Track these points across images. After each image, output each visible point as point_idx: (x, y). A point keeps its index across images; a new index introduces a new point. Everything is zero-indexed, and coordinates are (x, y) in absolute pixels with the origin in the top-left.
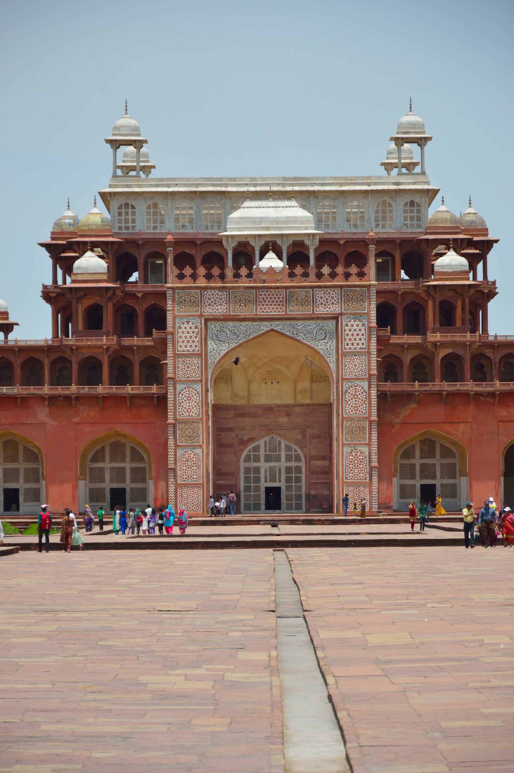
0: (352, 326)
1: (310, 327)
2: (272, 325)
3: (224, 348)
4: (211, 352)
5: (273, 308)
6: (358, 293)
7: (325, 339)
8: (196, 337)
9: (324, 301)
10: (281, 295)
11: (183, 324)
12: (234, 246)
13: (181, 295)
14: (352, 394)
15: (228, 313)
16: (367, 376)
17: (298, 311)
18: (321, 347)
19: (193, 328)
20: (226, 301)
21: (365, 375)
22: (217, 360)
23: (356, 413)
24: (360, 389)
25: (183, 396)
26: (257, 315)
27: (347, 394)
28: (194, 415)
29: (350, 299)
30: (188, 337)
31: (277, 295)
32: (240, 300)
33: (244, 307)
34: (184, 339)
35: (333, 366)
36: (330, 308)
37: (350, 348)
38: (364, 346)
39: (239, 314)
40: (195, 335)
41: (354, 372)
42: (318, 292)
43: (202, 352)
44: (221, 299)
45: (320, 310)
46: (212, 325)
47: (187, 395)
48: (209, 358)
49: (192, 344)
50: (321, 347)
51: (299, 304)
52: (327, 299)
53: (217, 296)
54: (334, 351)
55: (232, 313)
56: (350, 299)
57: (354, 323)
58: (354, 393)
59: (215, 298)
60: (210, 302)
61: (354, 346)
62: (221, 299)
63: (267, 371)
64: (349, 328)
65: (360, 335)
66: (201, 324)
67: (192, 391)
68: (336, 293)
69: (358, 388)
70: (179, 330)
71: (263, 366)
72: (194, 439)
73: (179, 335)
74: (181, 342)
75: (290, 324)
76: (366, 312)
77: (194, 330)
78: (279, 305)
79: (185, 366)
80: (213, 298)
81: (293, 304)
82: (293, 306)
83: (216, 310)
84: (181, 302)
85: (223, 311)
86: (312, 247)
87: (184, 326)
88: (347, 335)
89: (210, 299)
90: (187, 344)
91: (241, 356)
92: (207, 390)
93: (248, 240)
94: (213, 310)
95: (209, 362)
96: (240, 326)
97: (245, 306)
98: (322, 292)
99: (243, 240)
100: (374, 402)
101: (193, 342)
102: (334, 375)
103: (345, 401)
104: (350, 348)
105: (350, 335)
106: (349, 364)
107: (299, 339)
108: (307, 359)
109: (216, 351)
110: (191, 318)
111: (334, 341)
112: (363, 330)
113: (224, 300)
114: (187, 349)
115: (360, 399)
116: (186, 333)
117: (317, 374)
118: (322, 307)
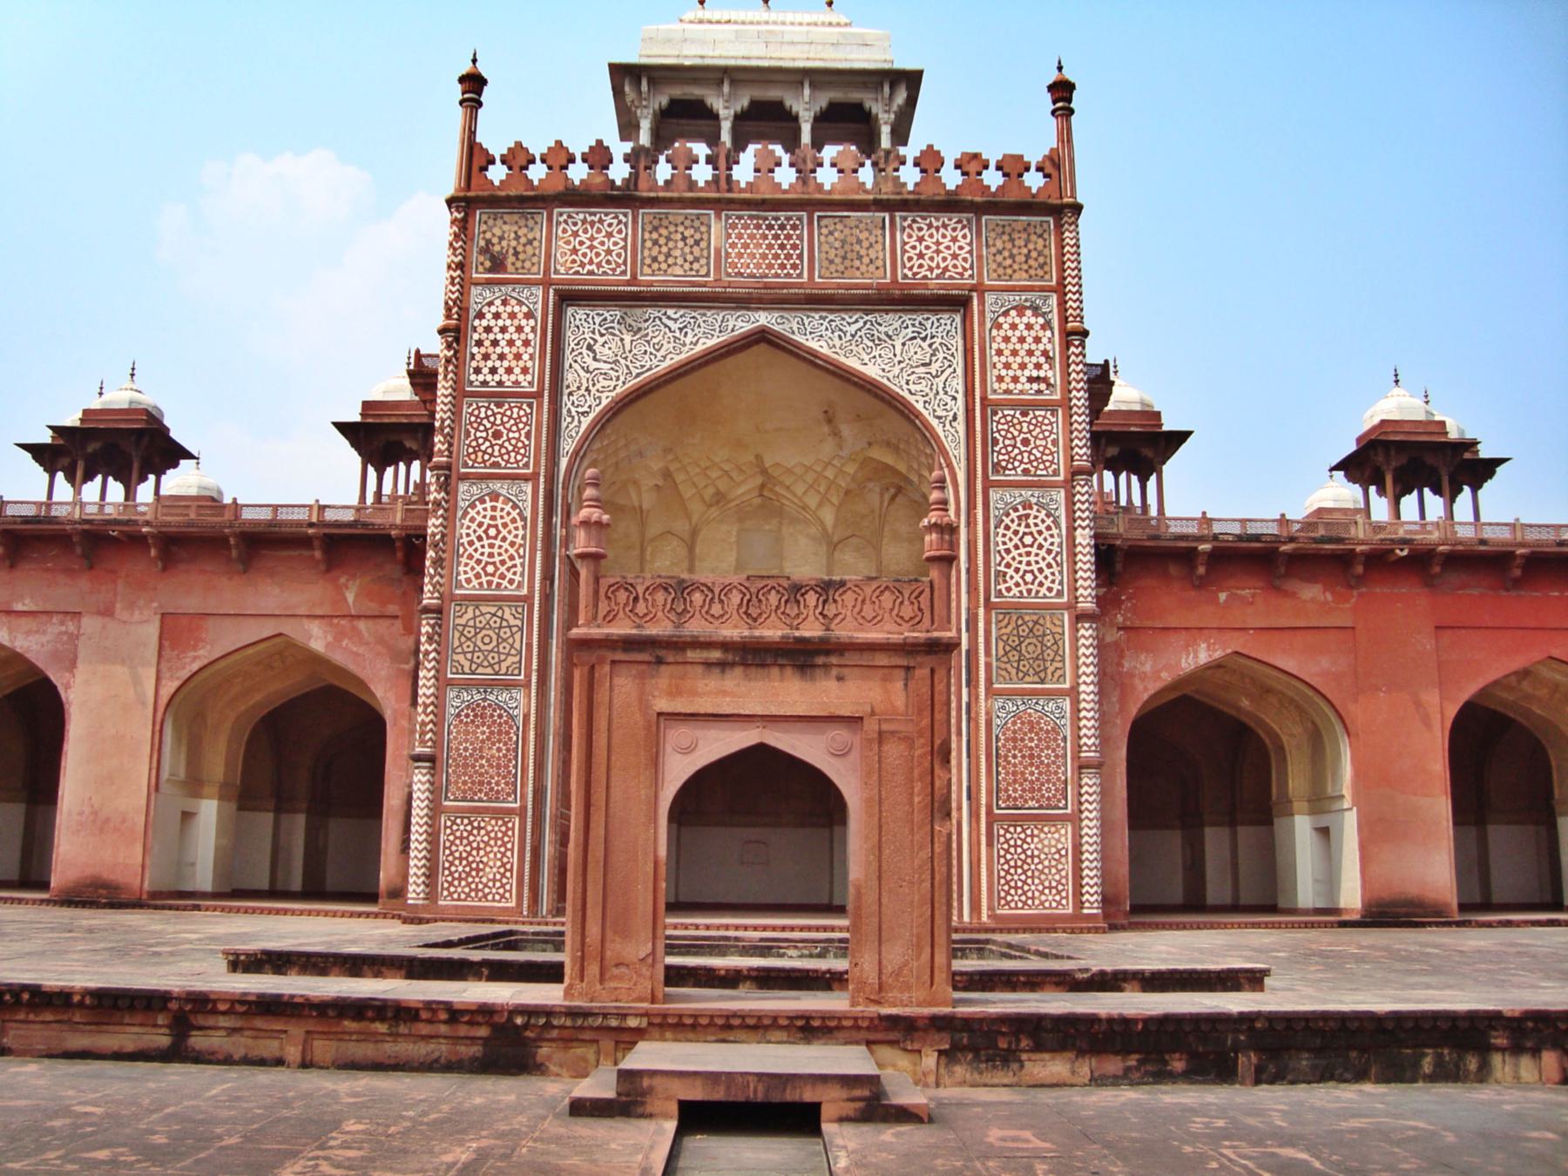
1: (882, 329)
9: (927, 248)
10: (794, 227)
11: (490, 304)
18: (918, 388)
19: (520, 316)
23: (1029, 591)
27: (1001, 531)
28: (505, 583)
34: (491, 350)
45: (915, 274)
46: (576, 315)
48: (564, 411)
50: (918, 388)
52: (938, 243)
70: (477, 322)
72: (499, 662)
88: (1000, 353)
94: (582, 265)
95: (564, 425)
100: (1086, 559)
106: (1005, 437)
109: (587, 389)
111: (960, 371)
113: (617, 237)
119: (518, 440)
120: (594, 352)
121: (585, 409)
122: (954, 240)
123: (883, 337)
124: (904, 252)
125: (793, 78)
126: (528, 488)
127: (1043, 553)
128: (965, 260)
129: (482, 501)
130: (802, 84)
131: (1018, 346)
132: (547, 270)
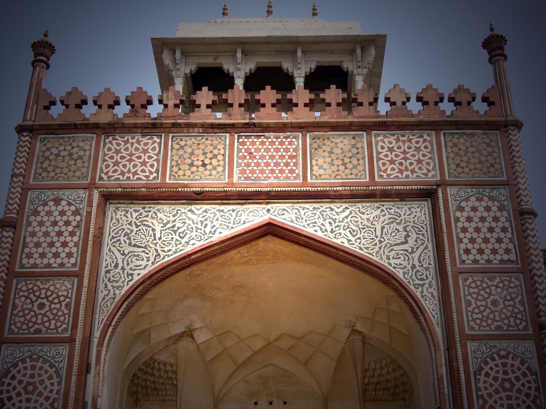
0: (474, 209)
1: (365, 217)
2: (268, 210)
3: (144, 263)
4: (108, 272)
5: (272, 171)
6: (480, 140)
7: (406, 242)
8: (72, 234)
10: (290, 143)
11: (45, 204)
12: (188, 71)
13: (49, 145)
14: (495, 379)
15: (159, 181)
16: (531, 331)
17: (335, 178)
18: (398, 261)
19: (69, 213)
20: (157, 155)
21: (526, 328)
22: (123, 292)
24: (517, 363)
25: (15, 383)
26: (232, 184)
27: (482, 378)
29: (462, 153)
30: (53, 234)
31: (282, 143)
32: (192, 153)
33: (201, 169)
34: (42, 240)
35: (431, 306)
36: (413, 171)
37: (475, 261)
38: (513, 257)
39: (186, 182)
40: (70, 228)
41: (494, 320)
42: (381, 137)
43: (82, 268)
44: (145, 151)
45: (389, 175)
47: (26, 379)
48: (101, 286)
49: (60, 250)
50: (398, 261)
51: (336, 162)
53: (136, 145)
54: (432, 271)
55: (168, 181)
56: (462, 153)
57: (477, 204)
58: (500, 376)
59: (132, 150)
60: (117, 158)
61: (485, 257)
62: (145, 151)
63: (260, 377)
64: (465, 214)
65: (498, 230)
66: (90, 205)
67: (41, 368)
68: (425, 140)
69: (510, 361)
70: (32, 218)
71: (248, 360)
73: (30, 229)
74: (31, 245)
75: (314, 209)
76: (505, 178)
77: (71, 218)
78: (287, 164)
79: (32, 302)
80: (127, 149)
81: (321, 162)
82: (321, 167)
83: (131, 175)
84: (47, 158)
85: (147, 177)
86: (360, 70)
87: (47, 208)
88: (464, 230)
89: (118, 152)
90: (47, 250)
91: (197, 325)
92: (85, 368)
93: (219, 61)
94: (123, 173)
95: (101, 296)
96: (189, 214)
97: (204, 165)
98: (392, 139)
99: (208, 61)
101: (65, 244)
102: (438, 331)
103: (478, 397)
104: (475, 261)
105: (471, 230)
107: (338, 241)
108: (354, 332)
110: (67, 192)
112: (503, 219)
114: (45, 261)
115: (519, 391)
116: (48, 224)
117: (375, 380)
118: (393, 169)
119: (59, 310)
120: (129, 239)
121: (120, 284)
122: (418, 149)
123: (365, 222)
124: (379, 159)
125: (290, 47)
126: (64, 350)
127: (522, 397)
128: (428, 164)
129: (24, 361)
130: (296, 52)
131: (480, 225)
132: (93, 178)
